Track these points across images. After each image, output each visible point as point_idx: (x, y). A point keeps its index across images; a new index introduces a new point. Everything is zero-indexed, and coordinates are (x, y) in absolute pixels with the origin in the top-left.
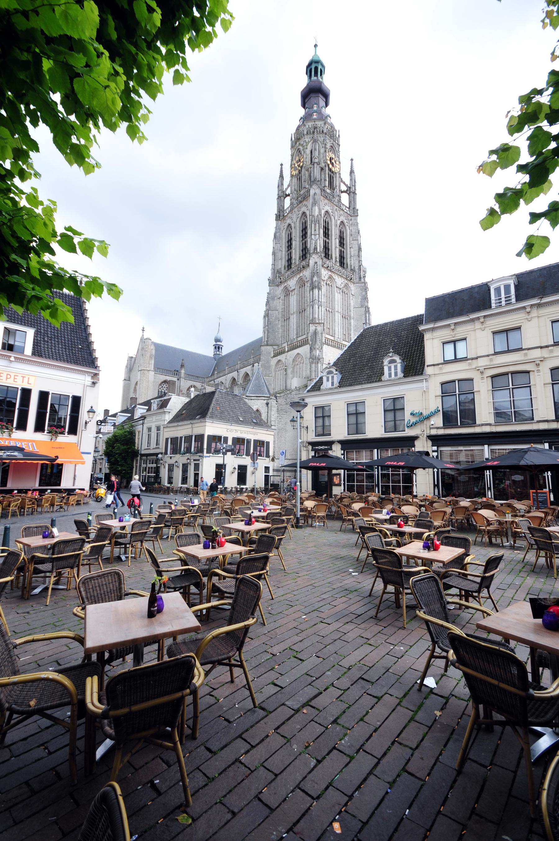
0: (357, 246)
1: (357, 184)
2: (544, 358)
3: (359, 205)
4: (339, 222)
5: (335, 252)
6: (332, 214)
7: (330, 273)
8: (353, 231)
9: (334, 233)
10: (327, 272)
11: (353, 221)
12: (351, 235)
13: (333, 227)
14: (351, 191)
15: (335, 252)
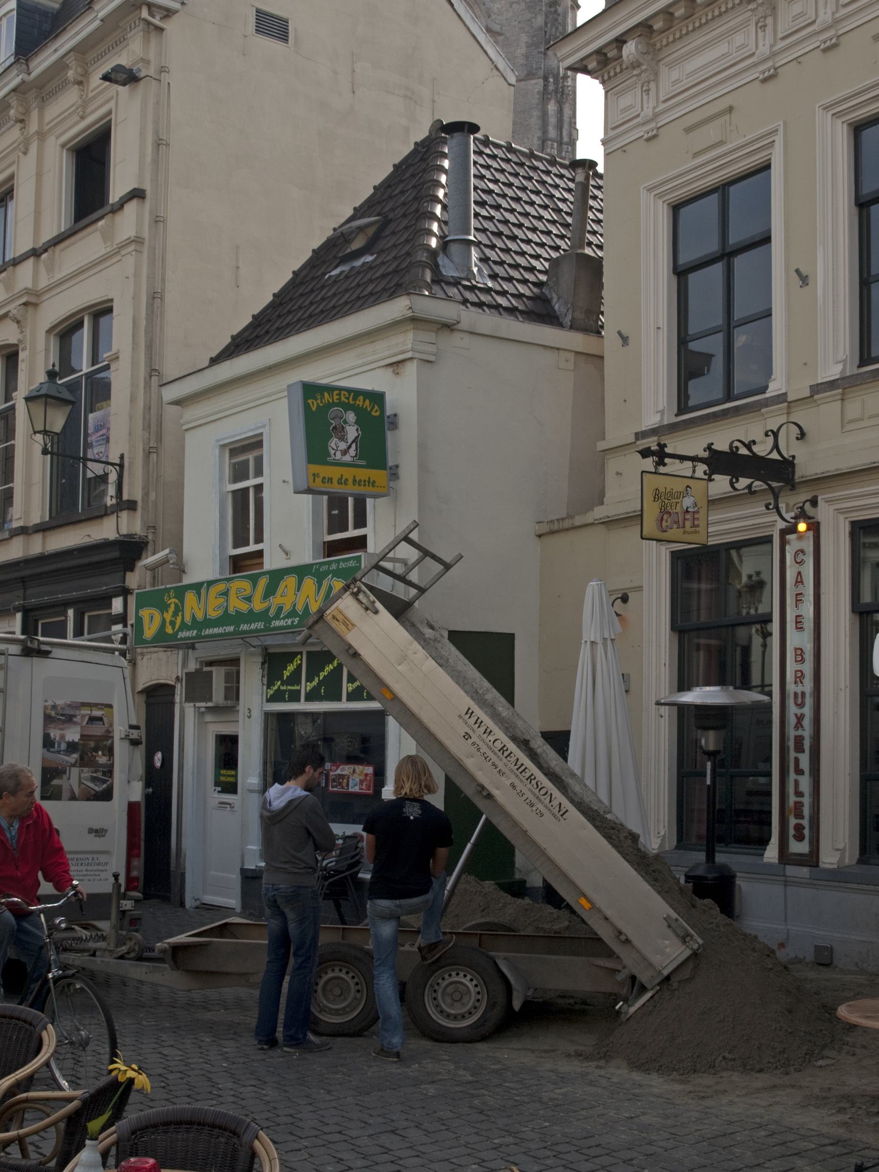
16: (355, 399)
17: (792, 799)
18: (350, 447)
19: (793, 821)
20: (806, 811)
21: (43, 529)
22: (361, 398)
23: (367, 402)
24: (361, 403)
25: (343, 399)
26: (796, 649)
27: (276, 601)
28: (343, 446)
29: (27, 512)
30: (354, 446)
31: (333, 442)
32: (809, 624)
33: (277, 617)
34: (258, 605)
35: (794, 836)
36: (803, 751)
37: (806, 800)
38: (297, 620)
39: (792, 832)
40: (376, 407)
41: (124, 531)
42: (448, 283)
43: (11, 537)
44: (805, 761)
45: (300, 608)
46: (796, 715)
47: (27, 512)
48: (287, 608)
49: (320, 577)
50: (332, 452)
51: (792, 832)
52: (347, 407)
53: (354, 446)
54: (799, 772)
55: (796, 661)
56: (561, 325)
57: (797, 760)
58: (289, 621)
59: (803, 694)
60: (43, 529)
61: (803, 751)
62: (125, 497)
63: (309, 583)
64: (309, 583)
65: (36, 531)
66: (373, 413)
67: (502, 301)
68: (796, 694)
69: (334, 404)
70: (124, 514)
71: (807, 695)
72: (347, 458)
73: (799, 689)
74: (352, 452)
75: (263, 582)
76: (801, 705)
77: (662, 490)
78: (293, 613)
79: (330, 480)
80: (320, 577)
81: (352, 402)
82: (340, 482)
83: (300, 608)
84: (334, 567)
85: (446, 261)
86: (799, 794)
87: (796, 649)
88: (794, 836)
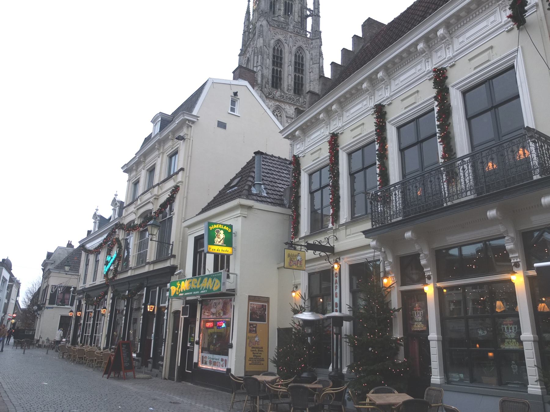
0: (317, 70)
1: (321, 7)
2: (158, 196)
3: (323, 27)
4: (294, 49)
5: (288, 80)
6: (285, 41)
7: (278, 103)
8: (314, 54)
9: (288, 60)
10: (273, 102)
11: (313, 44)
12: (312, 59)
13: (287, 55)
14: (316, 15)
15: (288, 80)
16: (223, 227)
18: (221, 240)
21: (154, 263)
22: (225, 227)
23: (227, 228)
24: (225, 228)
25: (220, 227)
27: (202, 285)
28: (219, 240)
29: (150, 258)
30: (222, 240)
31: (216, 239)
33: (202, 290)
34: (198, 287)
38: (206, 291)
40: (230, 229)
41: (172, 264)
42: (254, 195)
43: (146, 265)
45: (207, 288)
47: (150, 258)
48: (205, 287)
49: (213, 278)
50: (216, 242)
52: (221, 229)
53: (222, 240)
56: (285, 207)
58: (205, 291)
60: (154, 263)
62: (173, 254)
63: (210, 280)
64: (210, 280)
65: (152, 263)
66: (229, 231)
67: (269, 200)
69: (217, 228)
70: (172, 259)
72: (220, 244)
74: (222, 242)
75: (200, 279)
77: (290, 254)
78: (206, 289)
79: (215, 250)
80: (213, 278)
81: (222, 228)
82: (217, 250)
83: (207, 288)
84: (216, 275)
85: (254, 189)
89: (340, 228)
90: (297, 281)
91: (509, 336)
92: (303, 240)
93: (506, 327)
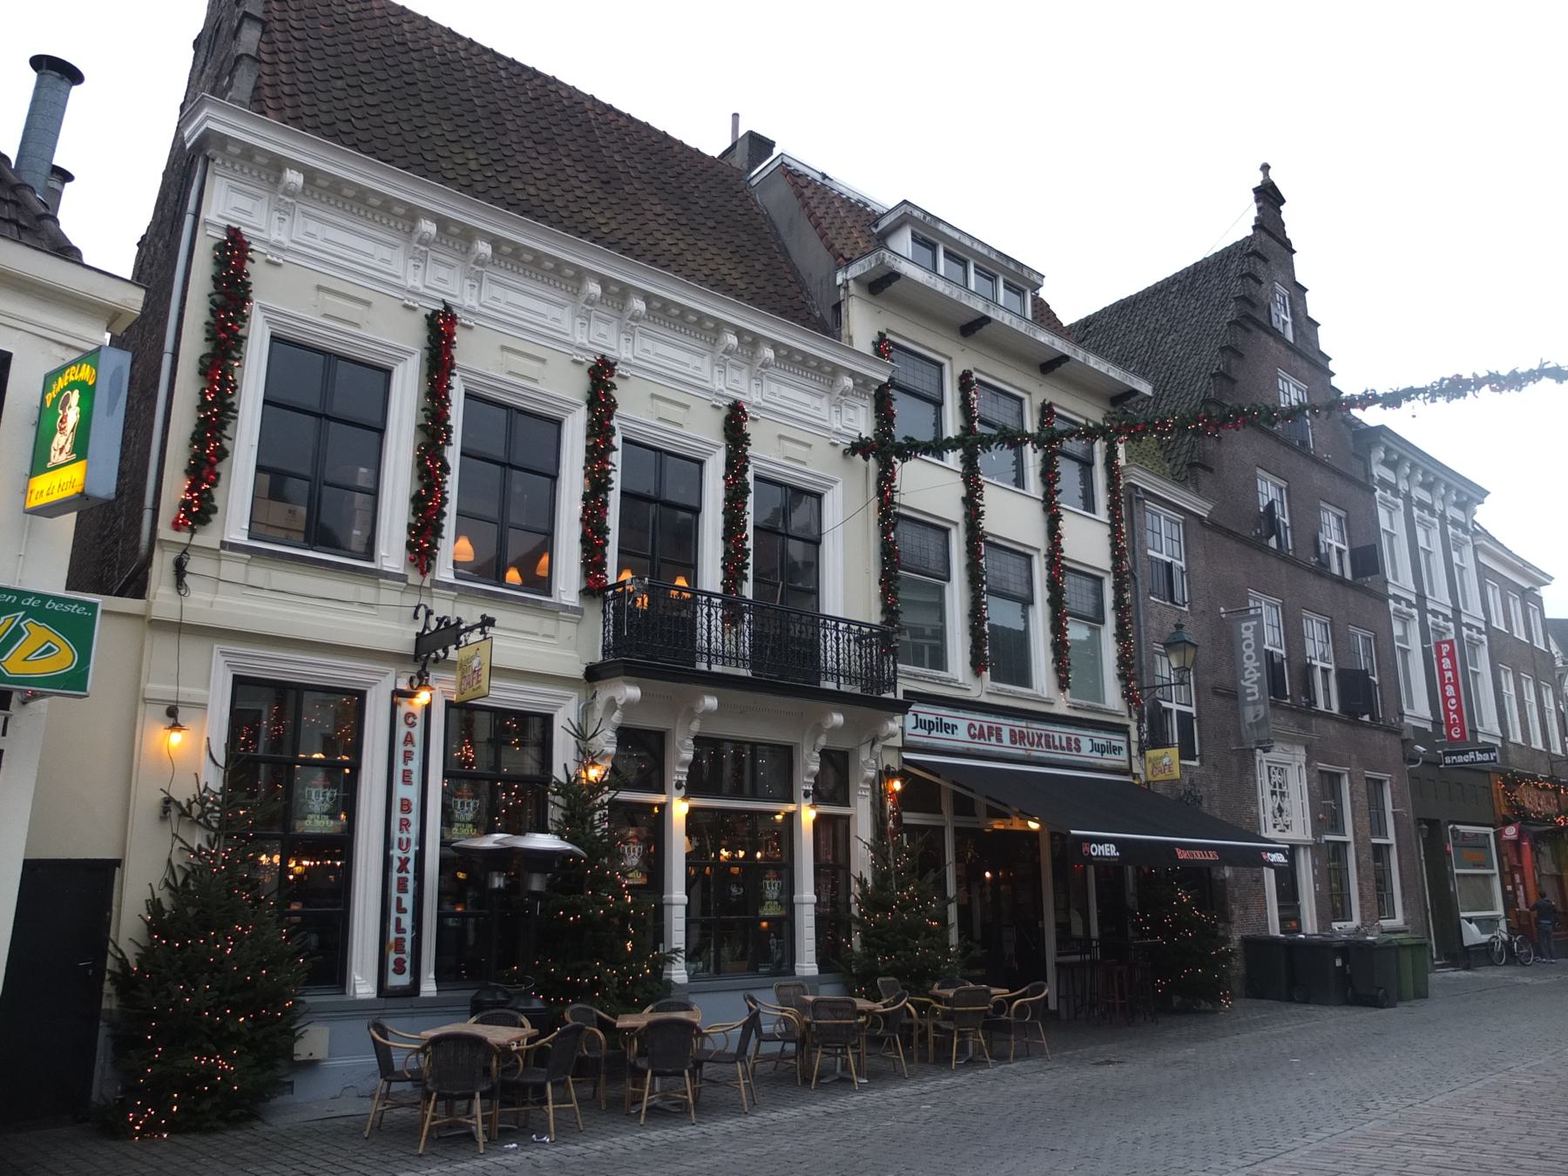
17: (393, 935)
19: (392, 956)
20: (408, 946)
26: (402, 800)
32: (416, 777)
35: (394, 970)
36: (406, 892)
37: (408, 936)
39: (391, 966)
44: (408, 901)
46: (400, 858)
51: (391, 966)
54: (401, 910)
55: (402, 810)
57: (399, 900)
59: (408, 840)
61: (406, 892)
68: (400, 839)
71: (413, 842)
73: (404, 836)
76: (406, 850)
86: (399, 930)
87: (402, 800)
88: (394, 970)
89: (434, 590)
90: (188, 692)
91: (770, 897)
92: (249, 557)
93: (768, 882)
